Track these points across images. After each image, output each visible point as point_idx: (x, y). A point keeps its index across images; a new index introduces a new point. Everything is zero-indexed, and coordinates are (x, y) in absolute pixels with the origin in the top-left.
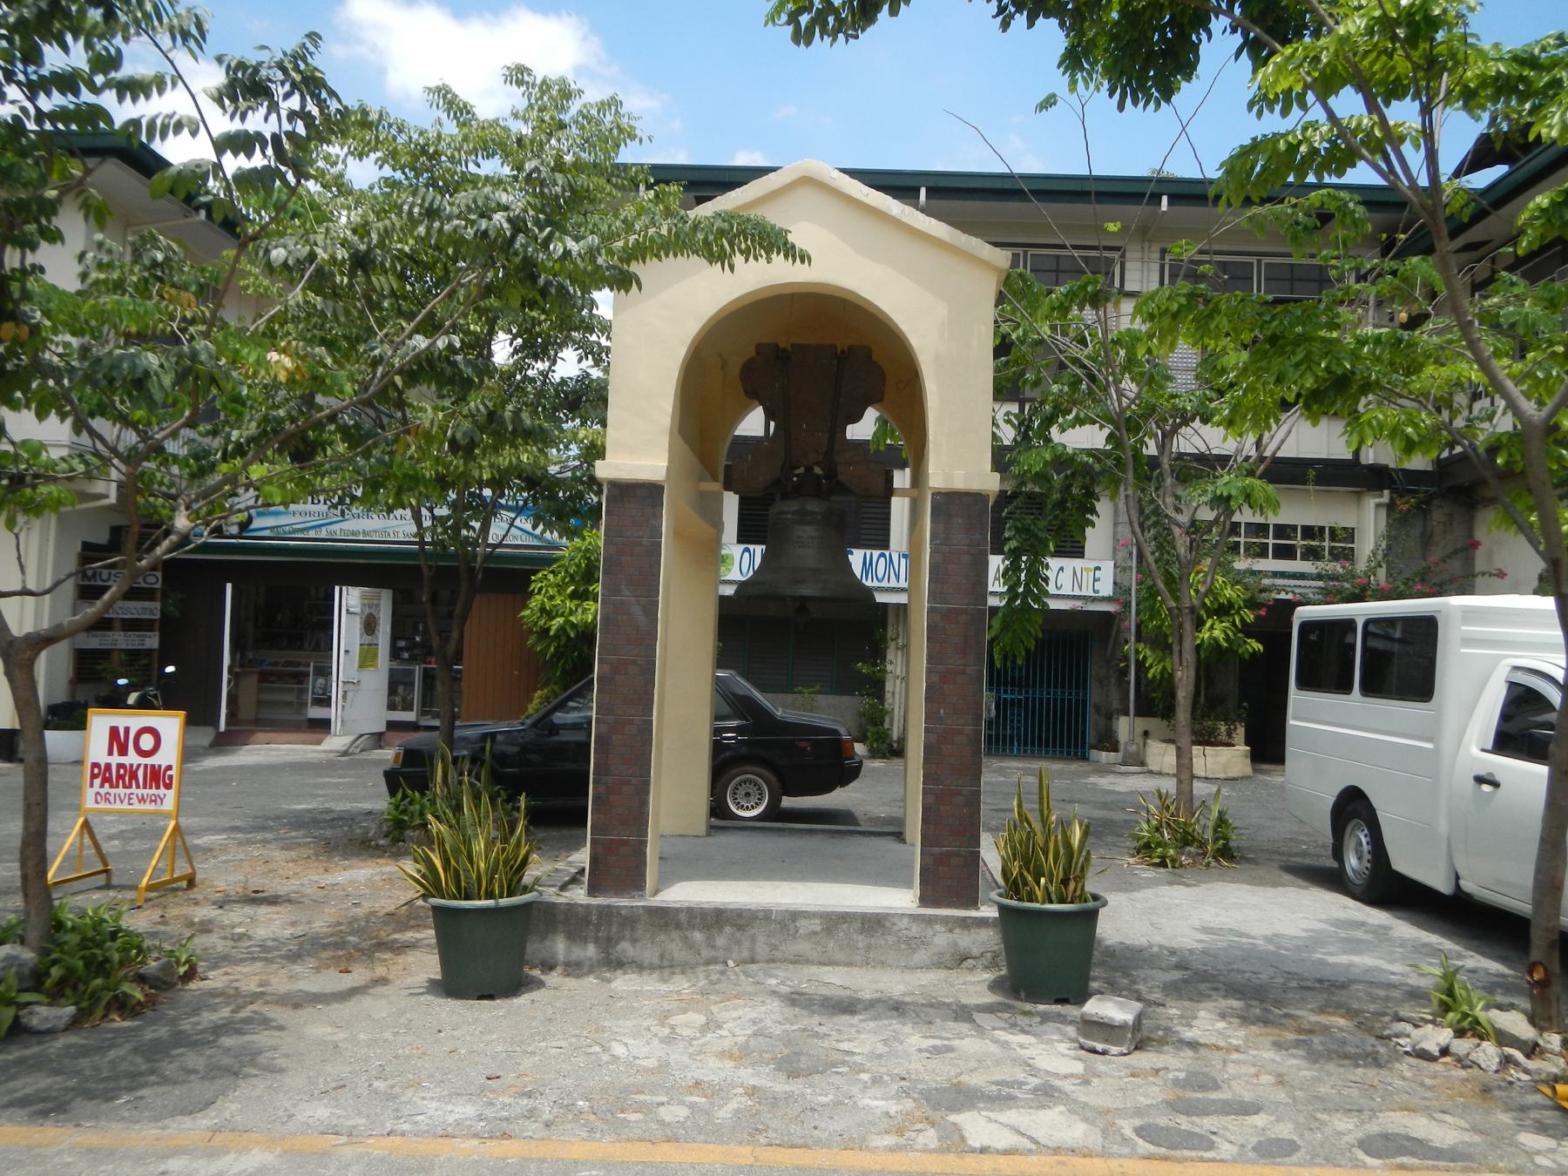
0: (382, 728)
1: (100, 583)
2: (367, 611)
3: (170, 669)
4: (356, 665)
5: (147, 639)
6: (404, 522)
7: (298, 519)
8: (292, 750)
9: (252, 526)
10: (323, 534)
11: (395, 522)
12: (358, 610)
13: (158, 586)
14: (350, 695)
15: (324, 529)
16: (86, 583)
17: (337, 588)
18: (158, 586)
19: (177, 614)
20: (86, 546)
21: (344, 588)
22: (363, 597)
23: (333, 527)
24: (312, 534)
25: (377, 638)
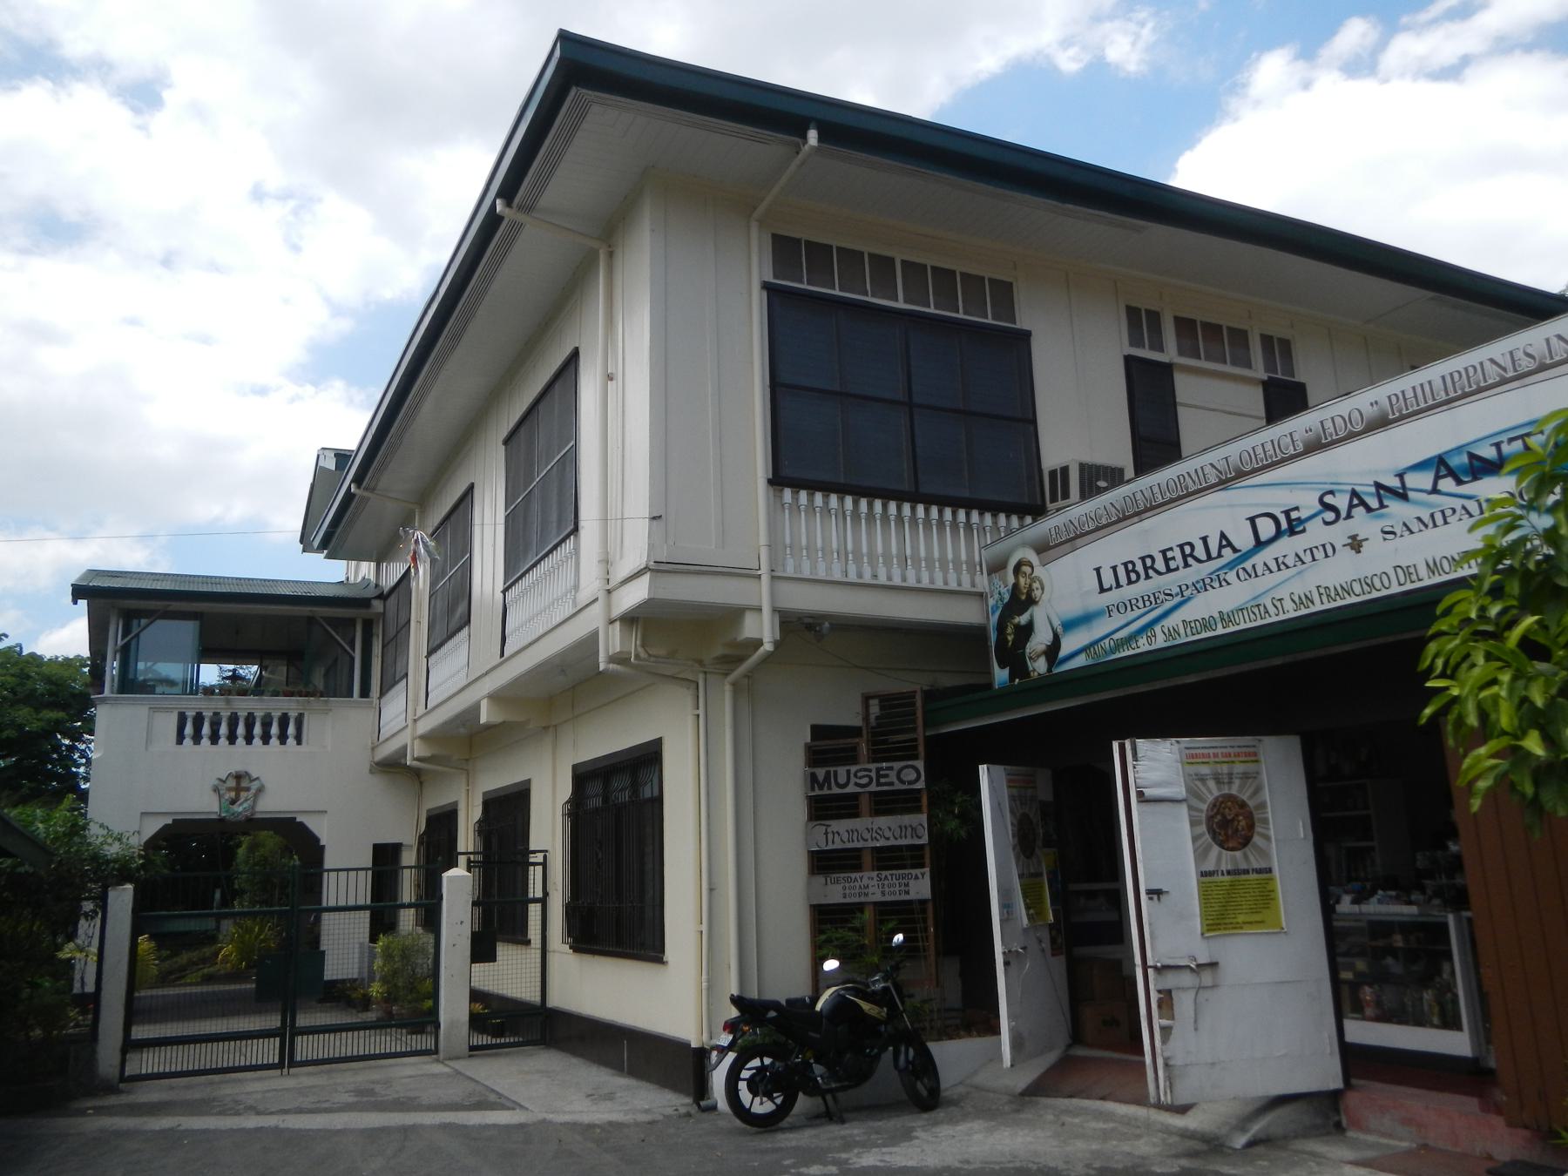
0: (1326, 1074)
1: (836, 790)
2: (1213, 791)
3: (899, 938)
4: (1197, 923)
5: (912, 882)
6: (1286, 573)
7: (1117, 620)
8: (1128, 1121)
9: (1063, 652)
10: (1160, 642)
11: (1267, 581)
12: (1179, 791)
13: (921, 785)
14: (1184, 1004)
15: (1158, 629)
16: (817, 792)
17: (1116, 745)
18: (921, 785)
19: (963, 833)
20: (818, 731)
21: (1128, 744)
22: (1190, 759)
23: (1170, 622)
24: (1143, 645)
25: (1265, 854)
